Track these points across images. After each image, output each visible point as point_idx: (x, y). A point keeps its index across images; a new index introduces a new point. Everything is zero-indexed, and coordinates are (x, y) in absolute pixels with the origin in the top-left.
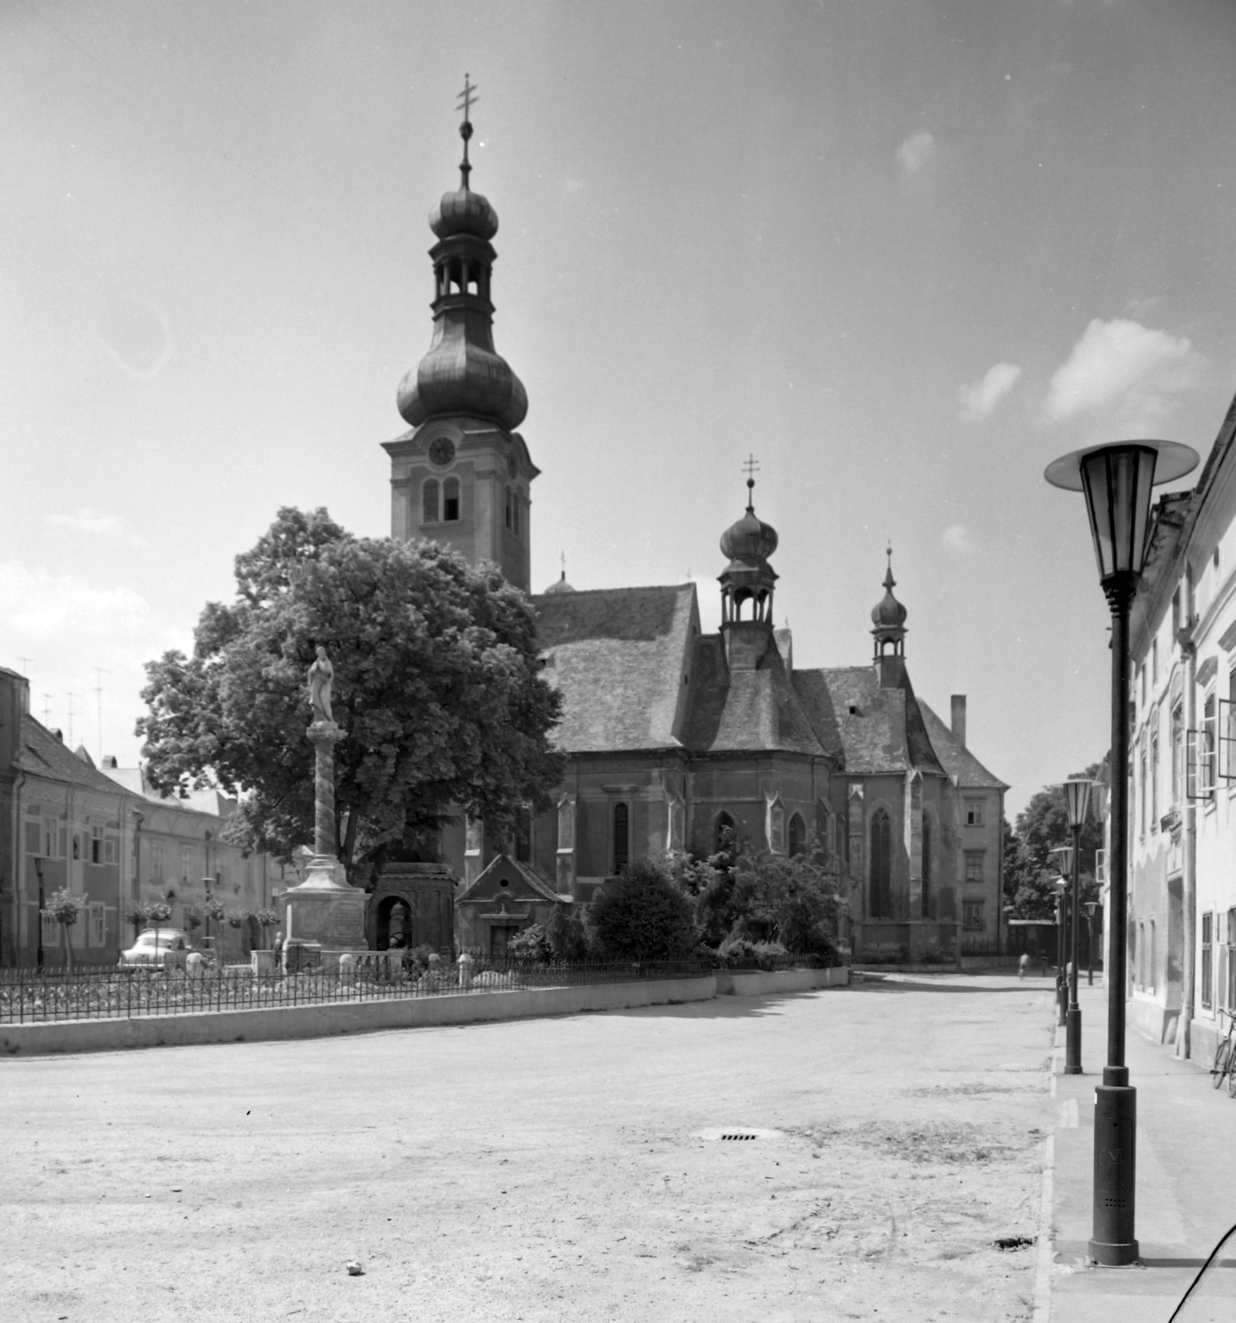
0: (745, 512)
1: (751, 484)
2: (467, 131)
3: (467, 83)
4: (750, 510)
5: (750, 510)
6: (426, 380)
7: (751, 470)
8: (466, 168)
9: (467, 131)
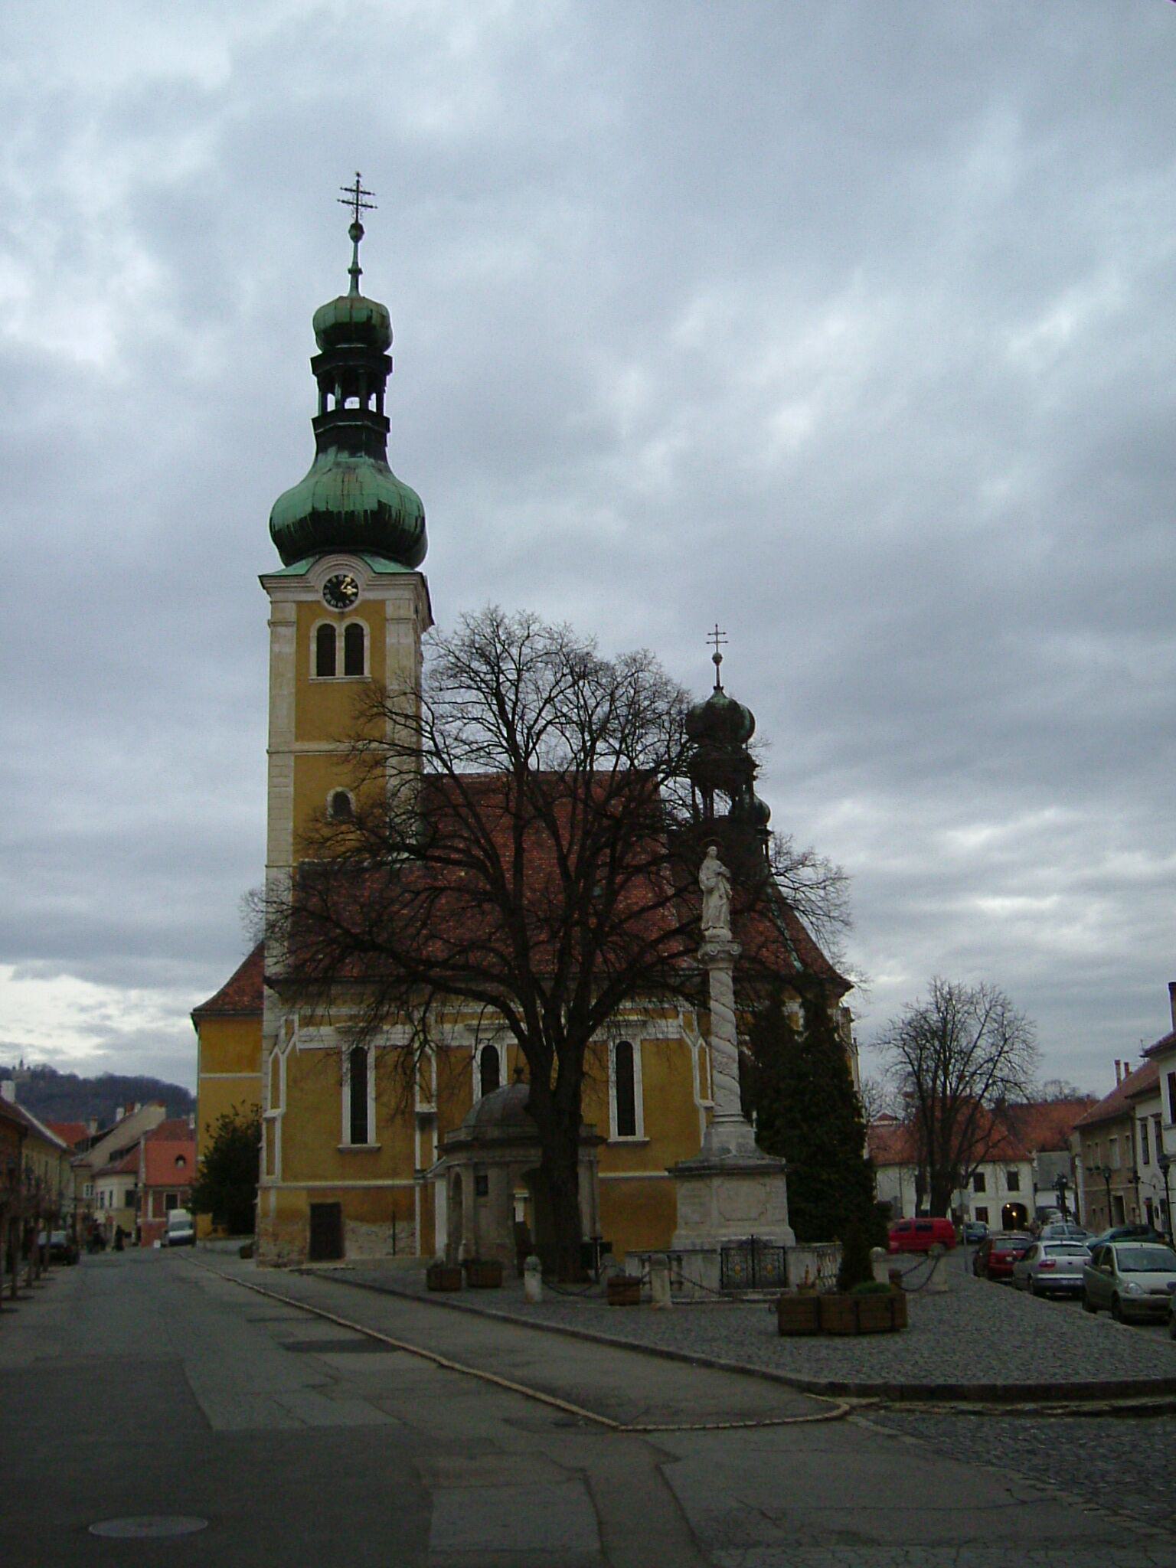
0: (712, 692)
1: (717, 659)
2: (357, 231)
3: (358, 182)
4: (718, 688)
5: (718, 688)
6: (322, 507)
7: (717, 642)
8: (355, 272)
9: (357, 231)
